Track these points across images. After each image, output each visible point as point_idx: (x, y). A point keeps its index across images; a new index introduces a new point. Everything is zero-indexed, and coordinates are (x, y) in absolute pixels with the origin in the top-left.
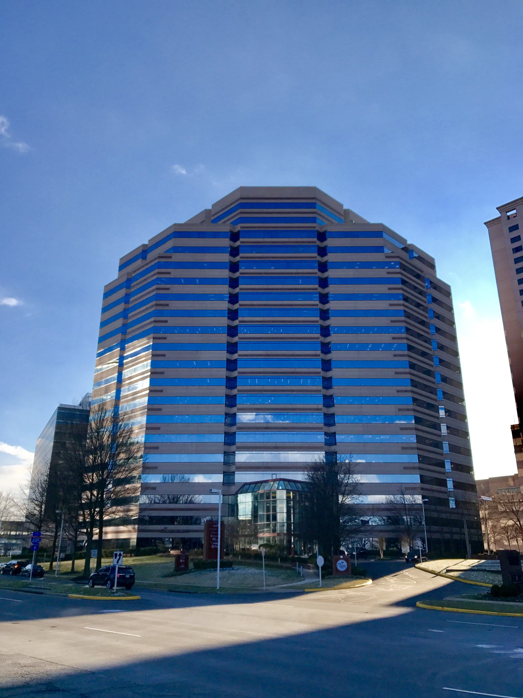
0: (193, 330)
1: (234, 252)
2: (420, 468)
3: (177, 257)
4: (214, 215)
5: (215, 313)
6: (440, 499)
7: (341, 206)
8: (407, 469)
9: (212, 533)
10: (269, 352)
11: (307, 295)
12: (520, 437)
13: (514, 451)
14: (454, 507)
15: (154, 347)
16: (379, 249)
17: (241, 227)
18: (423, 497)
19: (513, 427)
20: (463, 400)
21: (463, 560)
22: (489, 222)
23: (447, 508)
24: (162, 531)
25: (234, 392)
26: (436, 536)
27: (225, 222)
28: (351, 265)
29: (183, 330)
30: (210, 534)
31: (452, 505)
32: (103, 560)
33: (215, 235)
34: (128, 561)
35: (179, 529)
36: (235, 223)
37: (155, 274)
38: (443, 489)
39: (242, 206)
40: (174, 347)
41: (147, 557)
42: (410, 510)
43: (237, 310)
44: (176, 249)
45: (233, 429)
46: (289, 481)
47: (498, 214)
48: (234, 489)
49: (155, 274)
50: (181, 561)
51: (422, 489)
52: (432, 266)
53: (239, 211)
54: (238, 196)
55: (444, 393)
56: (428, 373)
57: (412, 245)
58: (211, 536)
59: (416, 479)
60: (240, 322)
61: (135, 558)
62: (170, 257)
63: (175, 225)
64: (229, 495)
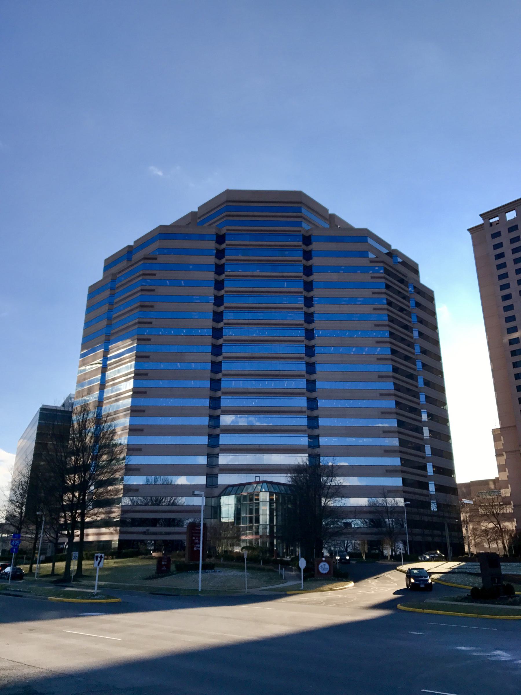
2: (403, 472)
3: (162, 259)
4: (200, 218)
6: (422, 502)
7: (327, 210)
8: (389, 472)
9: (194, 535)
12: (501, 441)
13: (495, 454)
14: (436, 510)
16: (363, 254)
17: (227, 230)
18: (405, 500)
19: (494, 431)
20: (445, 404)
21: (443, 562)
22: (472, 228)
23: (429, 511)
24: (144, 533)
26: (419, 538)
27: (210, 225)
28: (336, 269)
30: (193, 536)
31: (434, 508)
32: (84, 562)
33: (202, 237)
34: (111, 563)
35: (161, 531)
38: (425, 492)
42: (392, 512)
44: (161, 250)
47: (481, 221)
48: (217, 491)
50: (163, 563)
51: (404, 492)
52: (416, 271)
54: (224, 199)
55: (427, 397)
56: (412, 377)
57: (396, 251)
58: (194, 538)
59: (398, 482)
64: (213, 497)
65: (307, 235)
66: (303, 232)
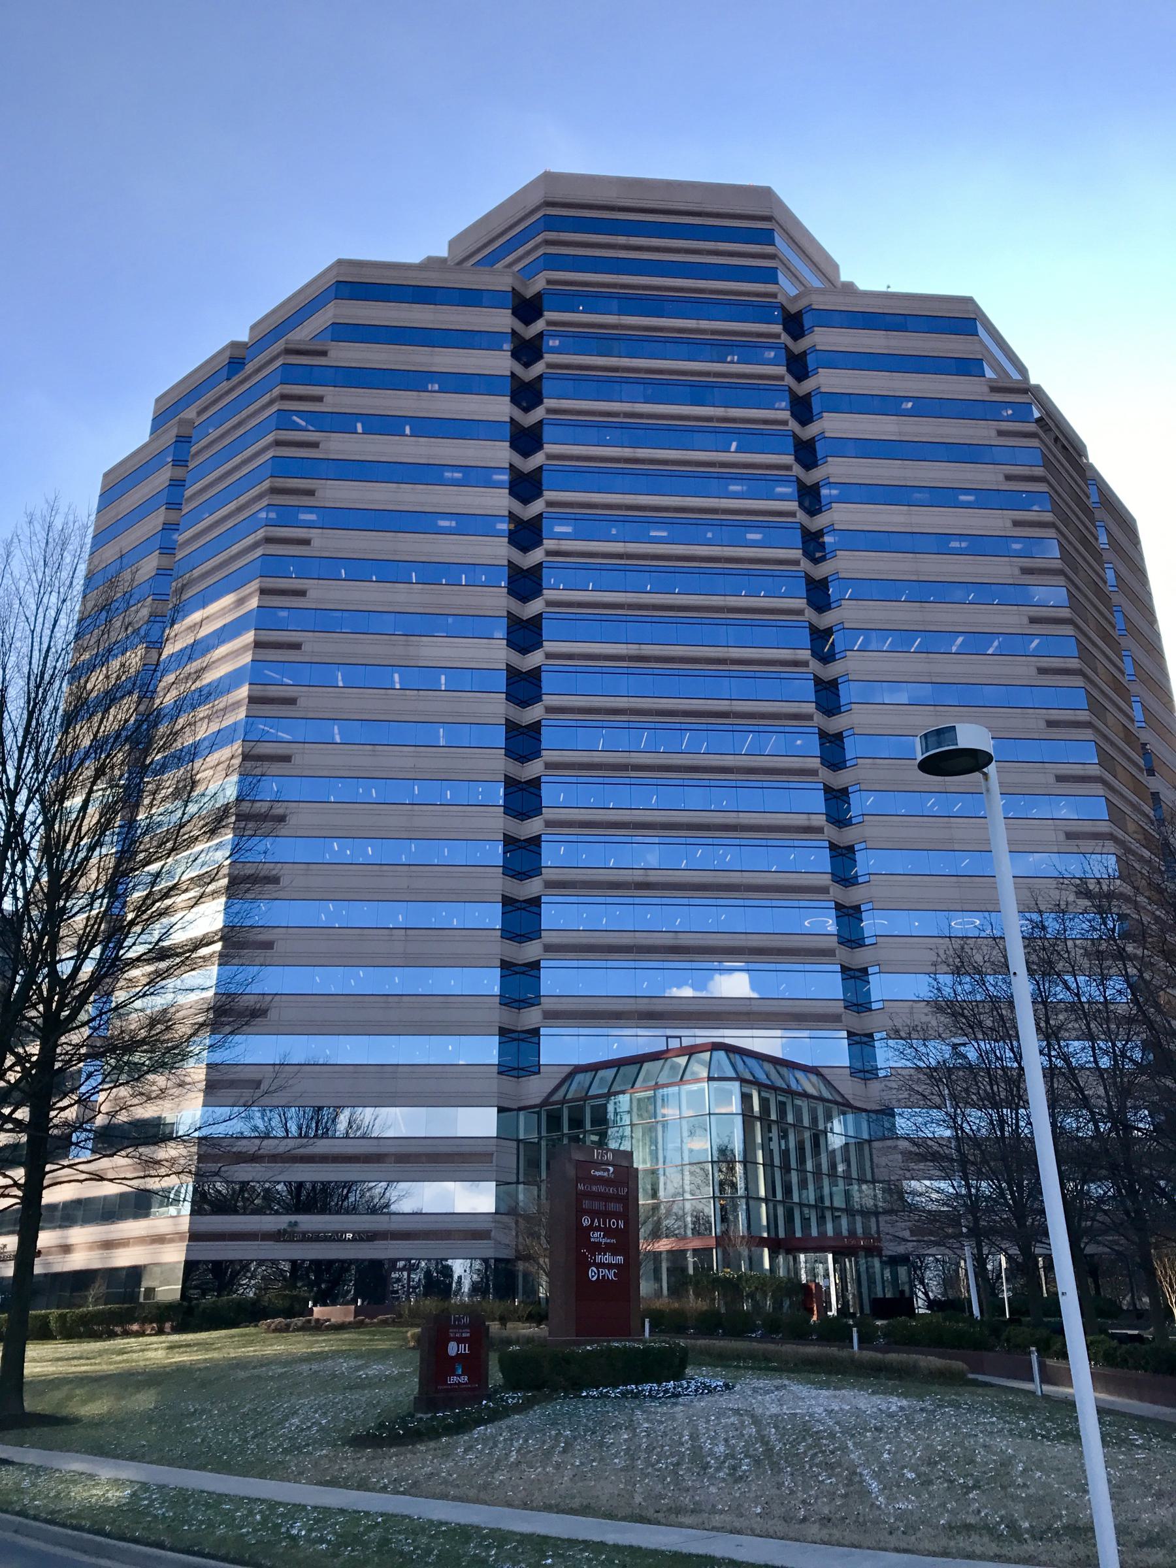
0: (390, 571)
1: (526, 351)
5: (470, 524)
10: (648, 650)
11: (759, 480)
15: (262, 619)
16: (968, 367)
17: (549, 282)
24: (278, 1236)
25: (534, 769)
28: (887, 405)
29: (361, 569)
32: (33, 1351)
34: (153, 1350)
36: (529, 273)
37: (271, 402)
39: (550, 223)
40: (329, 620)
41: (223, 1332)
43: (537, 620)
45: (531, 951)
46: (730, 1049)
49: (271, 402)
53: (539, 239)
54: (536, 199)
60: (549, 553)
61: (175, 1338)
62: (324, 353)
63: (340, 263)
64: (520, 1109)
65: (793, 309)
66: (781, 298)
